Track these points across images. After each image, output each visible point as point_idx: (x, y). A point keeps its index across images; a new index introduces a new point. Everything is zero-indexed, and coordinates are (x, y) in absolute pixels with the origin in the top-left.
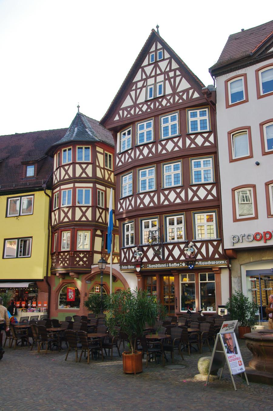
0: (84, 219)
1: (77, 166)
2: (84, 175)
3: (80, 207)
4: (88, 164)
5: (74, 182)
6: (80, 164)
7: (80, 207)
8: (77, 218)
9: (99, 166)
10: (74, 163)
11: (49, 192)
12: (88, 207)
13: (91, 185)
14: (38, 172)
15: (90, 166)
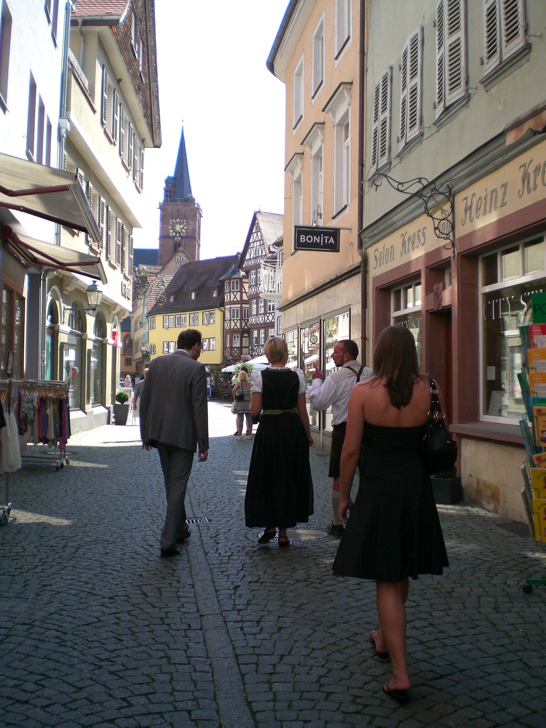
0: (236, 327)
1: (232, 293)
2: (235, 300)
3: (233, 320)
4: (238, 292)
5: (231, 304)
6: (233, 292)
7: (233, 320)
8: (232, 328)
9: (245, 292)
10: (230, 292)
11: (222, 308)
12: (238, 320)
13: (239, 306)
14: (219, 294)
15: (239, 293)
